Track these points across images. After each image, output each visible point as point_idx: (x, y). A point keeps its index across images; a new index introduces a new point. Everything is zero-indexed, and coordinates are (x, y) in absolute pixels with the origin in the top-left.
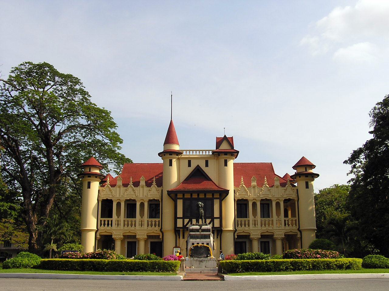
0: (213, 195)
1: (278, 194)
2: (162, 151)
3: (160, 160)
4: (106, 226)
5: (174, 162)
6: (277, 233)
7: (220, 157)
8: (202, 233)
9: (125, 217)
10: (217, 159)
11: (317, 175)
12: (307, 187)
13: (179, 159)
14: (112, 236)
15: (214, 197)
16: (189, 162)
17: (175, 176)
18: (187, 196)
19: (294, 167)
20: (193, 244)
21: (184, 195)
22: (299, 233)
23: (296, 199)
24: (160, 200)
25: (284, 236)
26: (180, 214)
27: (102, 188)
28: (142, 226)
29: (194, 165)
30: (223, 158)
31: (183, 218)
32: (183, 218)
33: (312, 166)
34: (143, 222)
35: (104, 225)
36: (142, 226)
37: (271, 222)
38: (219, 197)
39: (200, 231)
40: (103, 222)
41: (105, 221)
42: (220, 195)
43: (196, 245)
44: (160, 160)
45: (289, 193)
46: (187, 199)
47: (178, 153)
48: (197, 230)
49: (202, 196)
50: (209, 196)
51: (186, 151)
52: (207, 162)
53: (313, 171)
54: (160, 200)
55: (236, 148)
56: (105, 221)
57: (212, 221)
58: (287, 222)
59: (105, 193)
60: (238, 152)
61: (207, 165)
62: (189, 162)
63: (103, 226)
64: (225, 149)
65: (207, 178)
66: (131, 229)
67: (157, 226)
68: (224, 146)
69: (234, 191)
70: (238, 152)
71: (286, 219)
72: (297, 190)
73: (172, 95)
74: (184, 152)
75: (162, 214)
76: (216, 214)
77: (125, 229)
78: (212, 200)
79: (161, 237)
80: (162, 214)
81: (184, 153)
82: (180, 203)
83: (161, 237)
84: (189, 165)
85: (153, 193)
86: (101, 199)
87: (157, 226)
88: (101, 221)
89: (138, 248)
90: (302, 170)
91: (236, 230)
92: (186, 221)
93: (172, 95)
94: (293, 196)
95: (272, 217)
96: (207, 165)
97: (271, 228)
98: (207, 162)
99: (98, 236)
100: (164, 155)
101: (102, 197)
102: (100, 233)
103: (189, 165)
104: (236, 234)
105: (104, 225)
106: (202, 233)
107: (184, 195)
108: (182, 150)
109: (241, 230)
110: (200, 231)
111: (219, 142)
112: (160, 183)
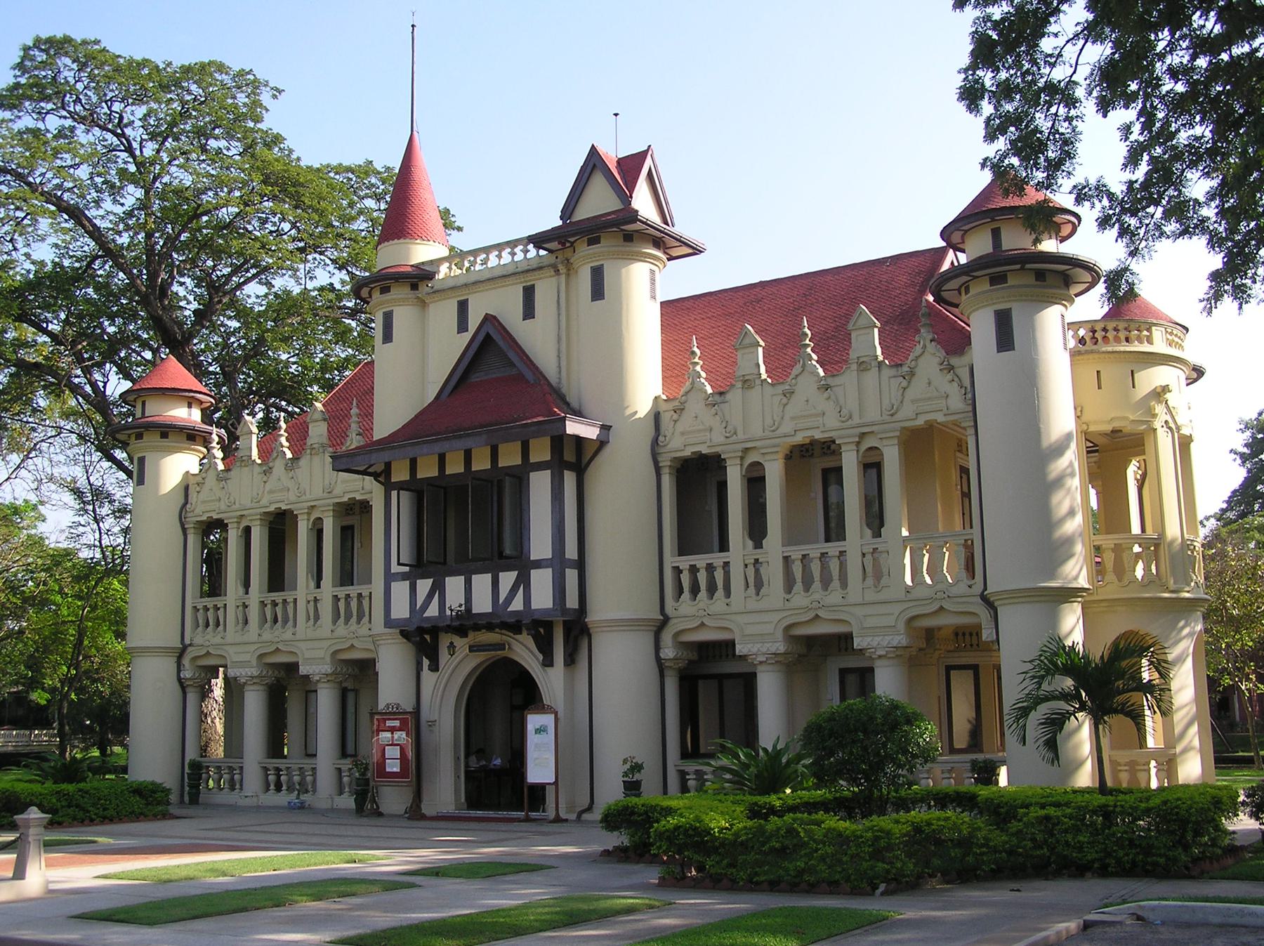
5: (404, 317)
6: (870, 622)
9: (260, 592)
12: (1005, 340)
13: (423, 304)
15: (532, 460)
16: (463, 307)
25: (781, 647)
29: (474, 322)
30: (585, 257)
34: (366, 603)
52: (529, 293)
57: (523, 581)
58: (797, 569)
62: (463, 307)
76: (540, 545)
91: (666, 620)
92: (424, 585)
95: (724, 547)
98: (529, 293)
101: (198, 511)
102: (195, 659)
104: (667, 637)
108: (431, 262)
109: (697, 617)
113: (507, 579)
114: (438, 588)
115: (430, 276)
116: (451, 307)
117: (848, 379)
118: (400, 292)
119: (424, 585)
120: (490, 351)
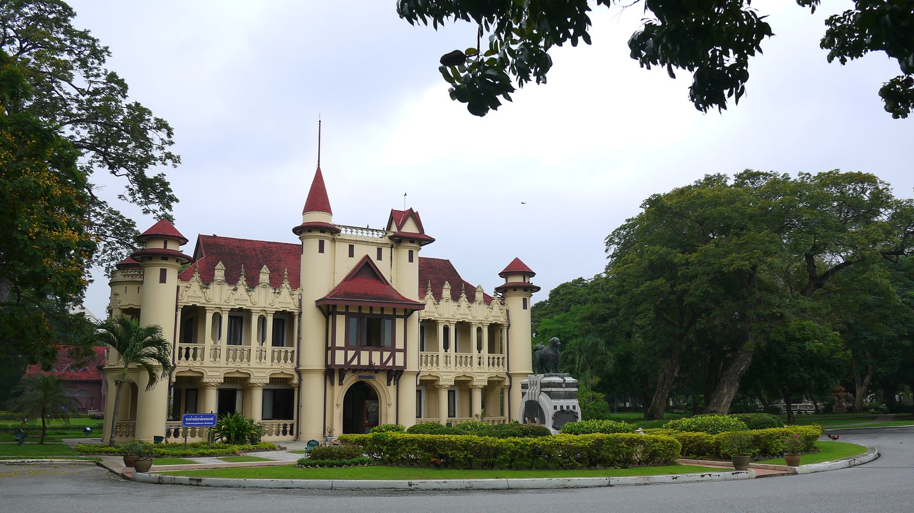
0: (394, 310)
1: (478, 314)
2: (299, 223)
3: (295, 240)
4: (191, 358)
5: (327, 244)
8: (567, 389)
11: (538, 289)
13: (334, 240)
14: (202, 377)
16: (351, 248)
17: (323, 272)
19: (502, 275)
20: (555, 407)
21: (347, 307)
22: (507, 379)
23: (506, 324)
26: (340, 341)
27: (183, 285)
28: (260, 359)
31: (346, 349)
32: (346, 349)
33: (532, 274)
35: (187, 357)
36: (260, 359)
37: (469, 360)
39: (564, 385)
40: (184, 351)
41: (188, 349)
43: (559, 409)
44: (295, 240)
45: (495, 314)
47: (333, 230)
48: (559, 385)
51: (346, 227)
52: (379, 251)
53: (533, 281)
55: (427, 232)
56: (188, 349)
57: (392, 355)
59: (190, 292)
61: (379, 258)
62: (351, 248)
63: (183, 358)
64: (405, 230)
66: (242, 366)
67: (289, 361)
68: (409, 228)
71: (491, 356)
72: (508, 311)
74: (343, 229)
75: (299, 339)
76: (399, 345)
77: (230, 365)
79: (295, 381)
80: (299, 339)
81: (343, 231)
82: (341, 321)
83: (295, 381)
84: (351, 254)
85: (285, 300)
86: (181, 305)
87: (289, 361)
88: (180, 349)
89: (169, 399)
90: (519, 280)
92: (351, 353)
94: (502, 320)
96: (379, 258)
97: (469, 370)
98: (379, 251)
99: (174, 380)
103: (351, 254)
105: (187, 357)
106: (567, 389)
107: (347, 307)
109: (427, 371)
110: (564, 385)
111: (397, 217)
112: (296, 283)
113: (386, 355)
114: (358, 354)
115: (338, 231)
116: (345, 247)
117: (475, 306)
118: (327, 235)
119: (351, 353)
120: (367, 268)
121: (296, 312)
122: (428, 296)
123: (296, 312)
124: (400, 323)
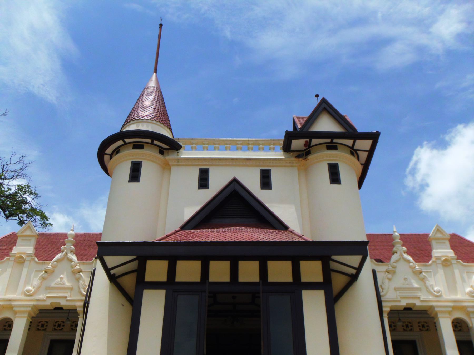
0: (296, 272)
7: (310, 157)
10: (305, 171)
18: (188, 271)
21: (172, 271)
24: (80, 309)
38: (320, 279)
42: (327, 271)
46: (188, 287)
49: (249, 272)
50: (280, 272)
54: (80, 309)
60: (374, 137)
61: (266, 182)
65: (269, 220)
69: (374, 272)
70: (374, 137)
73: (161, 25)
78: (297, 286)
84: (204, 182)
93: (161, 25)
96: (266, 182)
100: (117, 151)
103: (204, 182)
107: (172, 271)
121: (79, 305)
122: (394, 258)
123: (79, 305)
124: (313, 307)
